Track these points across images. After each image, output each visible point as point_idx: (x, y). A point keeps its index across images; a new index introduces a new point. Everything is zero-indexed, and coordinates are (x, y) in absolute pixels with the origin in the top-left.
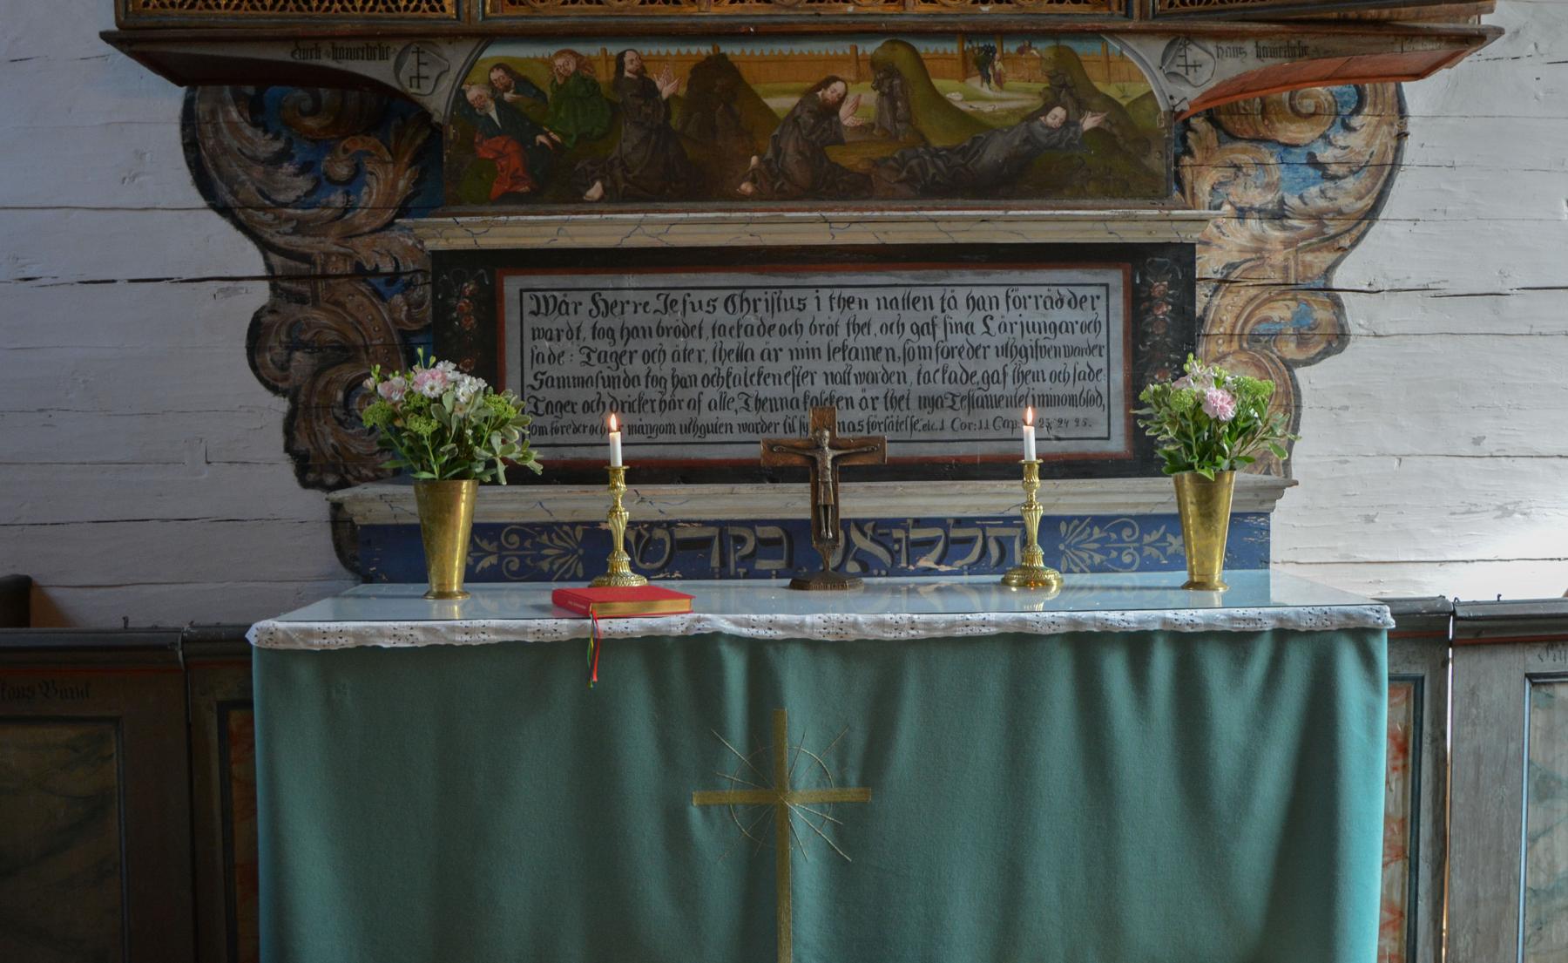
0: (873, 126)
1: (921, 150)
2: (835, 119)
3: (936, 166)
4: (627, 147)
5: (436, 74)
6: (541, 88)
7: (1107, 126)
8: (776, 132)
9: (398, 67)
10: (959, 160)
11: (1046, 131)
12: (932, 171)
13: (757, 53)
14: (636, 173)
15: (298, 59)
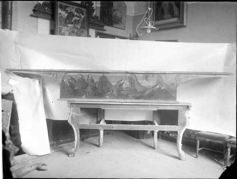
0: (128, 88)
1: (136, 92)
2: (122, 86)
3: (138, 94)
4: (89, 90)
5: (59, 77)
6: (76, 80)
7: (166, 89)
8: (113, 88)
9: (53, 76)
10: (141, 93)
11: (156, 89)
12: (137, 95)
13: (110, 75)
14: (90, 94)
15: (37, 74)
